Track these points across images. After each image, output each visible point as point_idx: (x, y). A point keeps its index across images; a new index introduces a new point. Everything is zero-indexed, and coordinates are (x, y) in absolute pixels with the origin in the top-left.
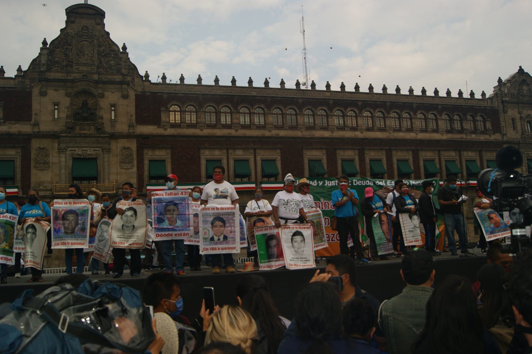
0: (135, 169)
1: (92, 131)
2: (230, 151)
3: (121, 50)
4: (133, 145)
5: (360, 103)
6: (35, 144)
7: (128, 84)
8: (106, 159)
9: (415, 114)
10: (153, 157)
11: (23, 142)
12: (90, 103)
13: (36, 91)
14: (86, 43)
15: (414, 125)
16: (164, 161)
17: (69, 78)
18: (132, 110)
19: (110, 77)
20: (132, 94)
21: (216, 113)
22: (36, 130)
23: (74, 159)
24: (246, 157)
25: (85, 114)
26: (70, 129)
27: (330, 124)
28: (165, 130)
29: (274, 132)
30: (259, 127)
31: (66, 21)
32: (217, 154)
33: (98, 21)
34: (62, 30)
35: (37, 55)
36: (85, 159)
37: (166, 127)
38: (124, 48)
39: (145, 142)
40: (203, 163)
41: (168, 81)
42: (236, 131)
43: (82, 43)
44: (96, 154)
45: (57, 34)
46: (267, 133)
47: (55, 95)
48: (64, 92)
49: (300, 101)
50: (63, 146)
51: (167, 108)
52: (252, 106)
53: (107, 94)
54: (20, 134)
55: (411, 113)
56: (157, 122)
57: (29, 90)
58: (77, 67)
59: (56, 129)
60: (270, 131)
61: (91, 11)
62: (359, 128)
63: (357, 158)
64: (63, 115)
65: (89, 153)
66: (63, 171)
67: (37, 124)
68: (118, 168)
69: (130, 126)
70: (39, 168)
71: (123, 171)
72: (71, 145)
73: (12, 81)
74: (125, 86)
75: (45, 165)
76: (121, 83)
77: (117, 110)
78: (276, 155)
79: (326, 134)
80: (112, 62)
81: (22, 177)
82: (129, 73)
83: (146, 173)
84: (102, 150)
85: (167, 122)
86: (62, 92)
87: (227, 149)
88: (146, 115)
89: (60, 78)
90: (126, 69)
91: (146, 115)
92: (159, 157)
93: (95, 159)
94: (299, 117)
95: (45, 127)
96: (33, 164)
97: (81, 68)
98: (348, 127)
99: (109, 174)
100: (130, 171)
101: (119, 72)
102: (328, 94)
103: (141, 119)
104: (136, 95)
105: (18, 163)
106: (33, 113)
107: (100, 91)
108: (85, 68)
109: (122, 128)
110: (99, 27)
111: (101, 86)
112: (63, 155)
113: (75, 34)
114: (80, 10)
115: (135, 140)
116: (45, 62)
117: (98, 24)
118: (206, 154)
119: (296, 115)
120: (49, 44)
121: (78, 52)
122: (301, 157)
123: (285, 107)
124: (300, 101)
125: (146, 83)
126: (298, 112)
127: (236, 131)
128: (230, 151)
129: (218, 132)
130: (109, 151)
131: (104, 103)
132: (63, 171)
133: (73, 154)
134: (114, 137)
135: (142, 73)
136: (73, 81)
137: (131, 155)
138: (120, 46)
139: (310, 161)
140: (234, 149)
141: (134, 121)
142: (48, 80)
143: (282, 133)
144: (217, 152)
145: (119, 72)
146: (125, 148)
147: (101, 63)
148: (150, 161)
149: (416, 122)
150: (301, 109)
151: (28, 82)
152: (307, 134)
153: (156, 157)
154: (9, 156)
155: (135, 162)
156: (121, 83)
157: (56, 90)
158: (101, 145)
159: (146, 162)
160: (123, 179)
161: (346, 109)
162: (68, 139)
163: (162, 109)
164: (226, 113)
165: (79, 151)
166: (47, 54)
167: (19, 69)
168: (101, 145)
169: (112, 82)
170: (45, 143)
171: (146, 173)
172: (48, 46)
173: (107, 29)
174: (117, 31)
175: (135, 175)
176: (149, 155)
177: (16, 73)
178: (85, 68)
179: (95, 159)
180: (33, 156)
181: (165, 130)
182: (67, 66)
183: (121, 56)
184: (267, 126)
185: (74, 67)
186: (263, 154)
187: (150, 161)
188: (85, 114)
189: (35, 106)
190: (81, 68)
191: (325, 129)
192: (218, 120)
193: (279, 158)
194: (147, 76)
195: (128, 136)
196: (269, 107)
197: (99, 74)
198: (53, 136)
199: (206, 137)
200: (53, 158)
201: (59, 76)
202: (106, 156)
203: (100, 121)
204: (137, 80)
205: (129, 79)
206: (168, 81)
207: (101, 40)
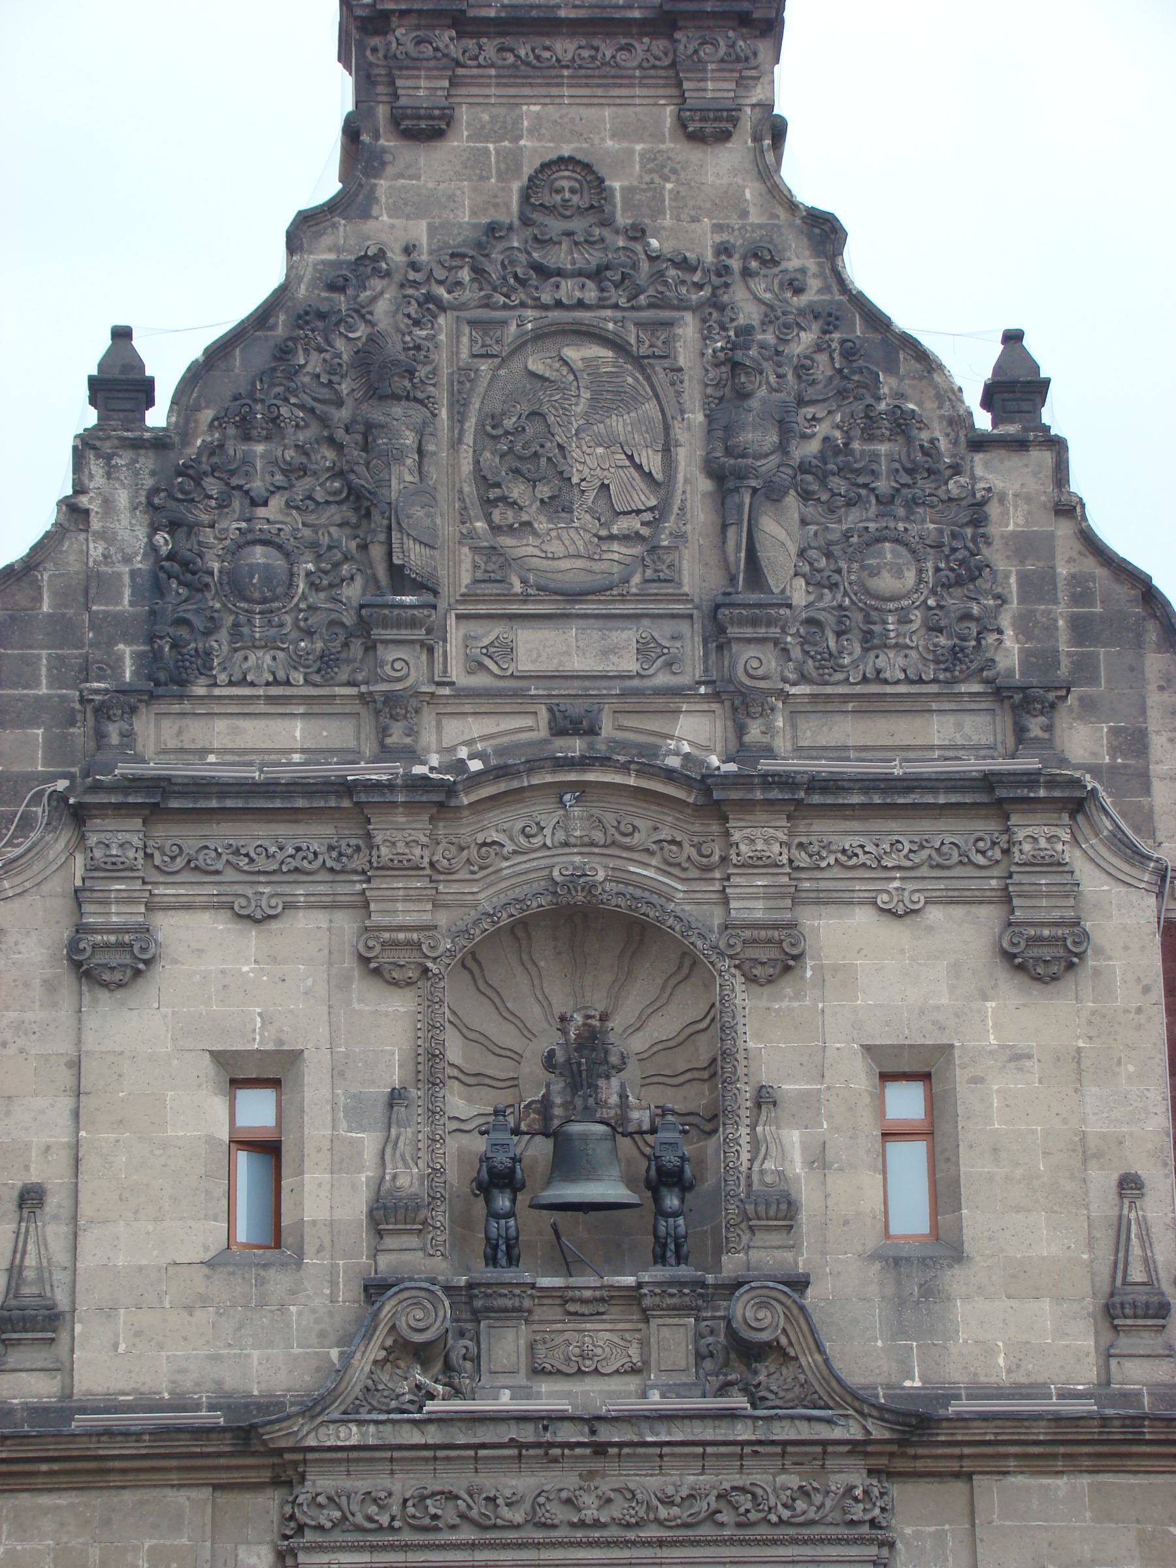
3: (983, 421)
12: (638, 1043)
31: (351, 132)
35: (41, 518)
38: (1018, 387)
45: (248, 273)
48: (346, 923)
58: (492, 633)
76: (996, 797)
89: (295, 767)
97: (541, 649)
111: (760, 836)
117: (707, 127)
120: (164, 394)
136: (437, 799)
138: (970, 370)
162: (403, 1484)
172: (157, 417)
173: (807, 176)
197: (739, 701)
201: (287, 739)
203: (762, 1254)
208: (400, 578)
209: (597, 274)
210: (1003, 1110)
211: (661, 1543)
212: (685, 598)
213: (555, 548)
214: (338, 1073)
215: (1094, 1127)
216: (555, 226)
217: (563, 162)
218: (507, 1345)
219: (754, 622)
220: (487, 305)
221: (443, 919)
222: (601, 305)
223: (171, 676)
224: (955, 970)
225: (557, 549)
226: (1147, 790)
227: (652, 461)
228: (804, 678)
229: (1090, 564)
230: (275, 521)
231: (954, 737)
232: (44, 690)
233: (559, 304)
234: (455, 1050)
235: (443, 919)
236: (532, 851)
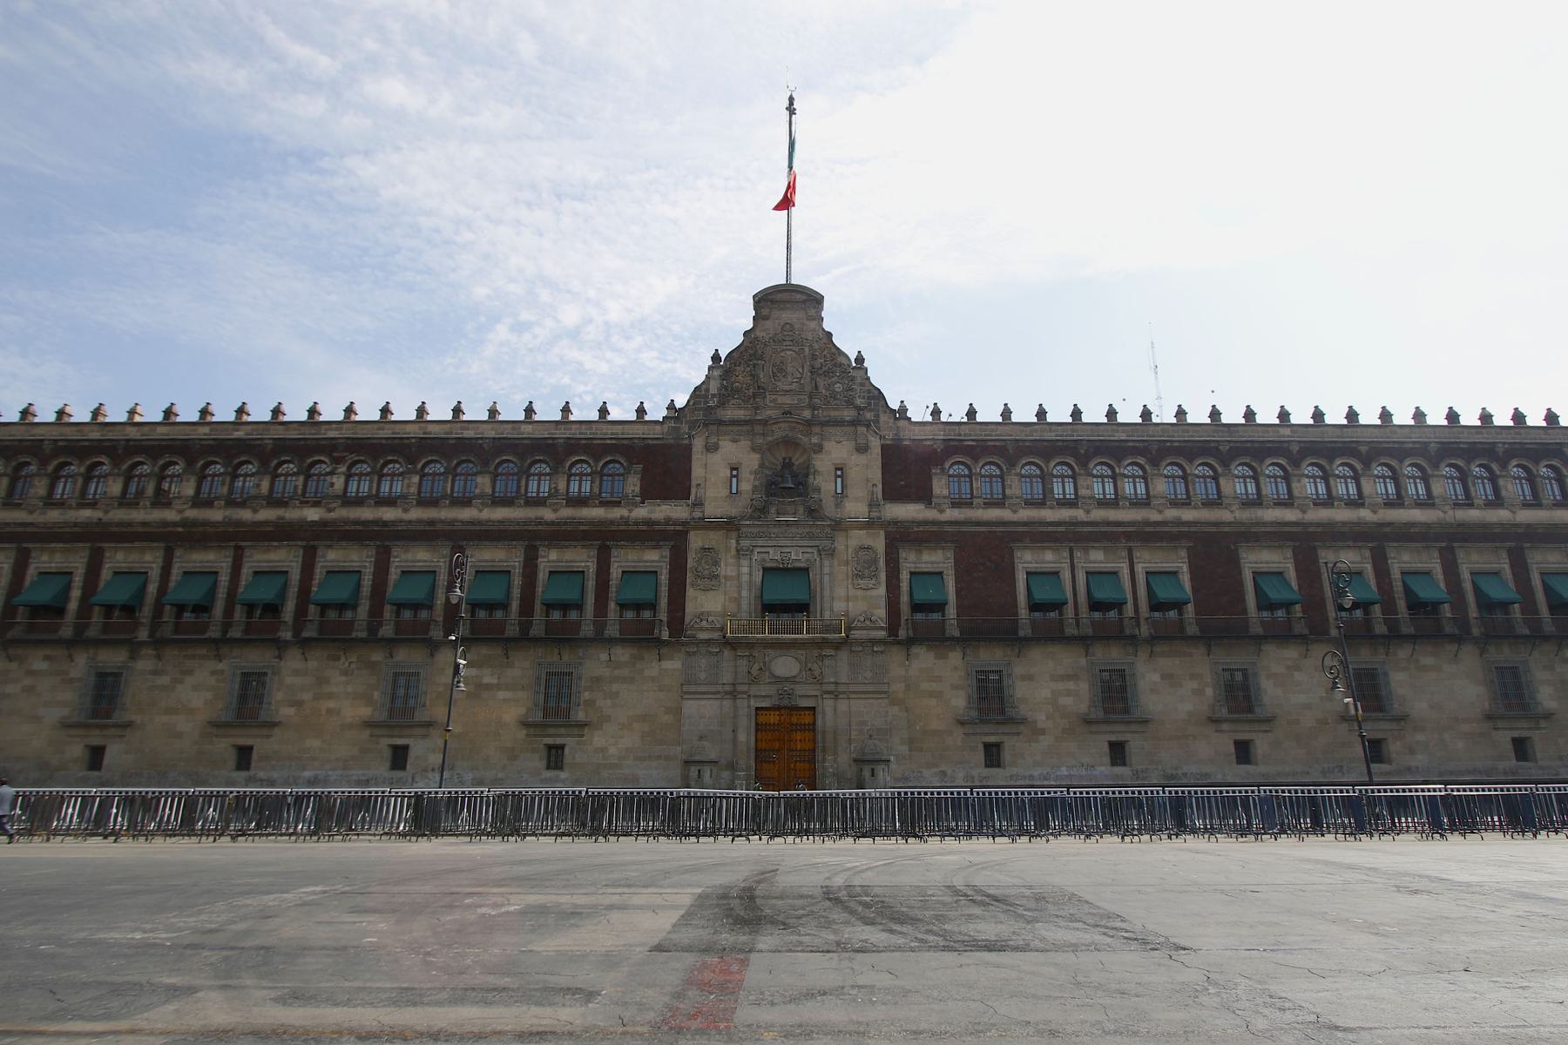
0: (882, 590)
1: (802, 514)
4: (879, 543)
5: (1363, 449)
6: (696, 540)
7: (868, 426)
8: (826, 570)
9: (1504, 466)
11: (673, 538)
13: (698, 444)
15: (1503, 493)
16: (940, 573)
18: (876, 475)
19: (833, 413)
20: (875, 444)
21: (1042, 477)
22: (697, 514)
23: (765, 569)
24: (1110, 566)
25: (787, 483)
26: (760, 511)
27: (1296, 493)
28: (942, 511)
29: (1171, 513)
30: (1136, 503)
32: (1049, 558)
33: (812, 312)
34: (746, 334)
36: (787, 569)
38: (860, 359)
39: (900, 537)
40: (1021, 578)
41: (944, 418)
42: (1088, 512)
46: (1154, 516)
47: (734, 450)
49: (1224, 448)
50: (745, 543)
51: (943, 470)
52: (1119, 461)
53: (826, 445)
54: (668, 521)
55: (1494, 466)
56: (923, 495)
59: (733, 512)
60: (1160, 512)
61: (799, 296)
62: (1367, 501)
63: (1369, 567)
64: (746, 487)
66: (745, 593)
67: (699, 504)
69: (872, 505)
71: (860, 593)
72: (760, 543)
73: (658, 427)
74: (862, 429)
75: (712, 580)
76: (854, 423)
77: (847, 472)
78: (1178, 562)
79: (1290, 515)
80: (838, 387)
83: (905, 598)
86: (745, 443)
93: (806, 570)
94: (1222, 481)
97: (780, 400)
98: (1340, 499)
99: (833, 599)
100: (873, 593)
101: (850, 403)
102: (1287, 432)
104: (883, 447)
105: (664, 578)
106: (694, 483)
107: (815, 440)
108: (788, 400)
110: (813, 324)
111: (816, 429)
112: (745, 562)
114: (779, 296)
115: (882, 533)
119: (1216, 478)
122: (1234, 563)
123: (1191, 461)
124: (1224, 448)
125: (901, 423)
126: (1220, 470)
127: (1088, 512)
128: (1077, 554)
129: (1048, 514)
130: (832, 553)
131: (823, 464)
132: (745, 593)
134: (838, 525)
135: (894, 404)
136: (764, 423)
137: (875, 561)
139: (1257, 575)
142: (721, 423)
143: (1188, 515)
144: (1049, 556)
145: (850, 403)
146: (862, 548)
147: (816, 387)
148: (912, 573)
149: (1510, 486)
150: (1226, 464)
151: (685, 428)
152: (1245, 515)
155: (883, 576)
156: (854, 423)
157: (734, 441)
158: (817, 543)
159: (905, 576)
160: (857, 608)
161: (1331, 460)
162: (756, 530)
164: (1063, 477)
165: (774, 555)
167: (671, 406)
168: (817, 543)
169: (839, 423)
170: (713, 538)
171: (905, 598)
174: (846, 329)
175: (883, 603)
176: (911, 560)
177: (665, 413)
178: (788, 400)
179: (806, 570)
180: (690, 564)
181: (942, 511)
182: (754, 396)
183: (853, 373)
184: (1154, 502)
186: (1148, 560)
187: (912, 573)
188: (787, 483)
189: (697, 472)
190: (780, 400)
191: (1288, 502)
192: (1047, 491)
193: (1185, 568)
194: (903, 409)
195: (870, 525)
196: (1155, 463)
197: (814, 408)
198: (729, 525)
199: (1025, 524)
200: (727, 568)
201: (740, 414)
202: (826, 563)
204: (883, 418)
205: (869, 415)
206: (944, 418)
207: (816, 346)
210: (853, 474)
223: (722, 404)
225: (782, 385)
231: (848, 414)
236: (779, 432)
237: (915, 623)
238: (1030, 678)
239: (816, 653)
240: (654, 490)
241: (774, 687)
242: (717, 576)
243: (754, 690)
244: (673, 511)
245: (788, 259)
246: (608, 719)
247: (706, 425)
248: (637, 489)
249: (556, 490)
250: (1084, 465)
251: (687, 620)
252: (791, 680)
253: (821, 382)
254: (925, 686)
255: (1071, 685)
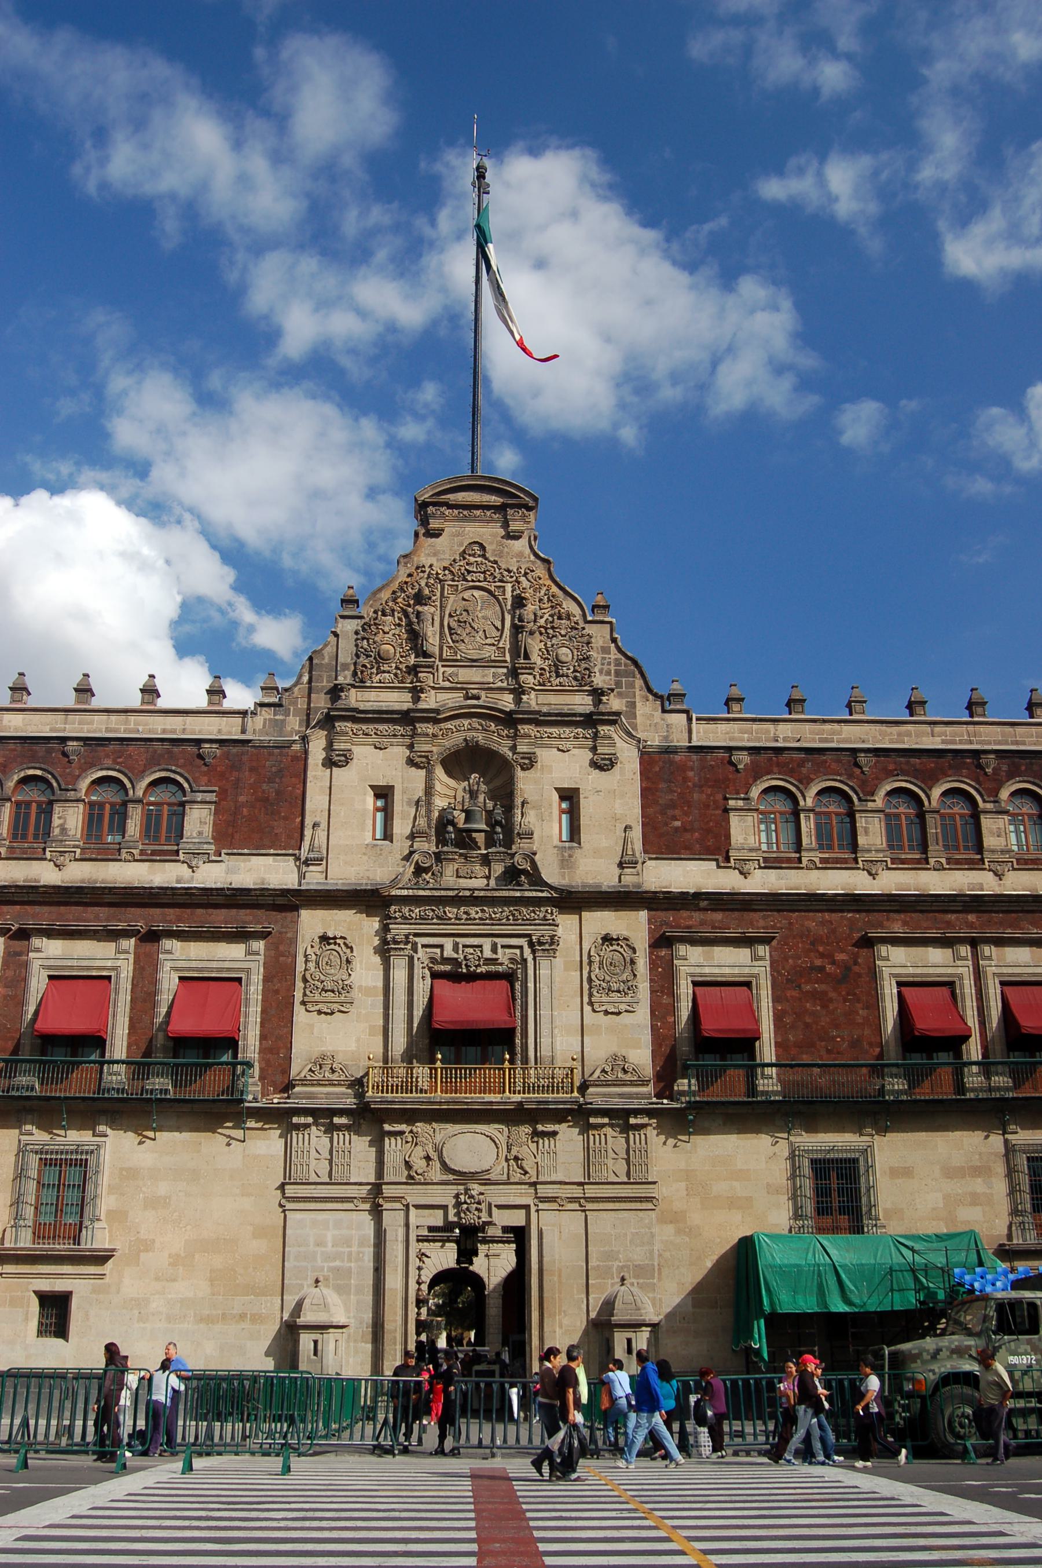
2: (987, 950)
4: (635, 926)
10: (707, 970)
14: (477, 593)
17: (422, 705)
18: (629, 807)
28: (744, 874)
32: (935, 961)
37: (751, 866)
40: (889, 991)
43: (467, 595)
44: (512, 960)
56: (717, 848)
57: (296, 747)
61: (494, 499)
65: (488, 953)
68: (587, 1008)
70: (320, 1007)
74: (603, 729)
81: (263, 1037)
82: (618, 684)
84: (531, 944)
85: (751, 850)
86: (399, 752)
87: (974, 943)
88: (678, 824)
89: (397, 707)
90: (608, 673)
91: (678, 824)
92: (727, 970)
95: (345, 870)
96: (298, 995)
97: (465, 675)
103: (663, 839)
105: (255, 990)
106: (309, 821)
109: (595, 869)
113: (445, 568)
116: (349, 660)
118: (897, 961)
121: (454, 624)
133: (433, 960)
136: (433, 717)
140: (1000, 942)
141: (638, 846)
142: (357, 716)
151: (294, 723)
153: (716, 971)
154: (227, 965)
155: (644, 987)
159: (685, 990)
163: (732, 803)
166: (357, 633)
169: (564, 719)
175: (646, 1037)
176: (695, 961)
185: (441, 670)
189: (315, 801)
190: (465, 675)
207: (525, 583)
208: (426, 655)
209: (484, 572)
211: (493, 925)
212: (505, 661)
213: (470, 647)
214: (404, 792)
215: (619, 811)
216: (472, 559)
217: (475, 542)
218: (450, 869)
219: (526, 668)
220: (453, 580)
221: (434, 749)
222: (485, 580)
223: (360, 683)
224: (581, 767)
226: (635, 718)
227: (499, 624)
228: (540, 685)
229: (620, 656)
230: (391, 639)
231: (582, 703)
232: (325, 684)
233: (473, 581)
234: (438, 787)
235: (434, 749)
237: (705, 1074)
238: (907, 1172)
239: (527, 1129)
240: (233, 835)
241: (453, 1189)
242: (347, 988)
243: (414, 1195)
244: (272, 871)
245: (474, 396)
246: (147, 1246)
247: (328, 722)
248: (208, 830)
249: (63, 830)
250: (993, 794)
251: (298, 1068)
252: (481, 1177)
253: (535, 645)
254: (721, 1188)
255: (978, 1185)
